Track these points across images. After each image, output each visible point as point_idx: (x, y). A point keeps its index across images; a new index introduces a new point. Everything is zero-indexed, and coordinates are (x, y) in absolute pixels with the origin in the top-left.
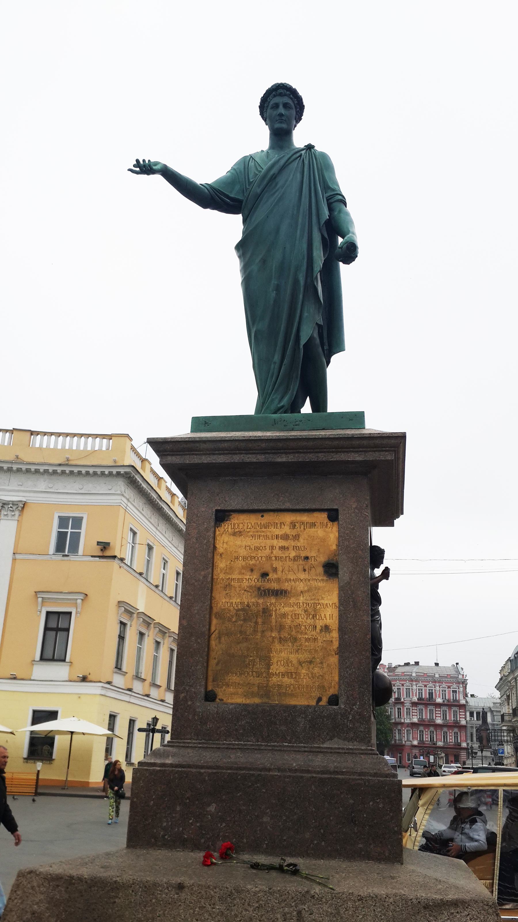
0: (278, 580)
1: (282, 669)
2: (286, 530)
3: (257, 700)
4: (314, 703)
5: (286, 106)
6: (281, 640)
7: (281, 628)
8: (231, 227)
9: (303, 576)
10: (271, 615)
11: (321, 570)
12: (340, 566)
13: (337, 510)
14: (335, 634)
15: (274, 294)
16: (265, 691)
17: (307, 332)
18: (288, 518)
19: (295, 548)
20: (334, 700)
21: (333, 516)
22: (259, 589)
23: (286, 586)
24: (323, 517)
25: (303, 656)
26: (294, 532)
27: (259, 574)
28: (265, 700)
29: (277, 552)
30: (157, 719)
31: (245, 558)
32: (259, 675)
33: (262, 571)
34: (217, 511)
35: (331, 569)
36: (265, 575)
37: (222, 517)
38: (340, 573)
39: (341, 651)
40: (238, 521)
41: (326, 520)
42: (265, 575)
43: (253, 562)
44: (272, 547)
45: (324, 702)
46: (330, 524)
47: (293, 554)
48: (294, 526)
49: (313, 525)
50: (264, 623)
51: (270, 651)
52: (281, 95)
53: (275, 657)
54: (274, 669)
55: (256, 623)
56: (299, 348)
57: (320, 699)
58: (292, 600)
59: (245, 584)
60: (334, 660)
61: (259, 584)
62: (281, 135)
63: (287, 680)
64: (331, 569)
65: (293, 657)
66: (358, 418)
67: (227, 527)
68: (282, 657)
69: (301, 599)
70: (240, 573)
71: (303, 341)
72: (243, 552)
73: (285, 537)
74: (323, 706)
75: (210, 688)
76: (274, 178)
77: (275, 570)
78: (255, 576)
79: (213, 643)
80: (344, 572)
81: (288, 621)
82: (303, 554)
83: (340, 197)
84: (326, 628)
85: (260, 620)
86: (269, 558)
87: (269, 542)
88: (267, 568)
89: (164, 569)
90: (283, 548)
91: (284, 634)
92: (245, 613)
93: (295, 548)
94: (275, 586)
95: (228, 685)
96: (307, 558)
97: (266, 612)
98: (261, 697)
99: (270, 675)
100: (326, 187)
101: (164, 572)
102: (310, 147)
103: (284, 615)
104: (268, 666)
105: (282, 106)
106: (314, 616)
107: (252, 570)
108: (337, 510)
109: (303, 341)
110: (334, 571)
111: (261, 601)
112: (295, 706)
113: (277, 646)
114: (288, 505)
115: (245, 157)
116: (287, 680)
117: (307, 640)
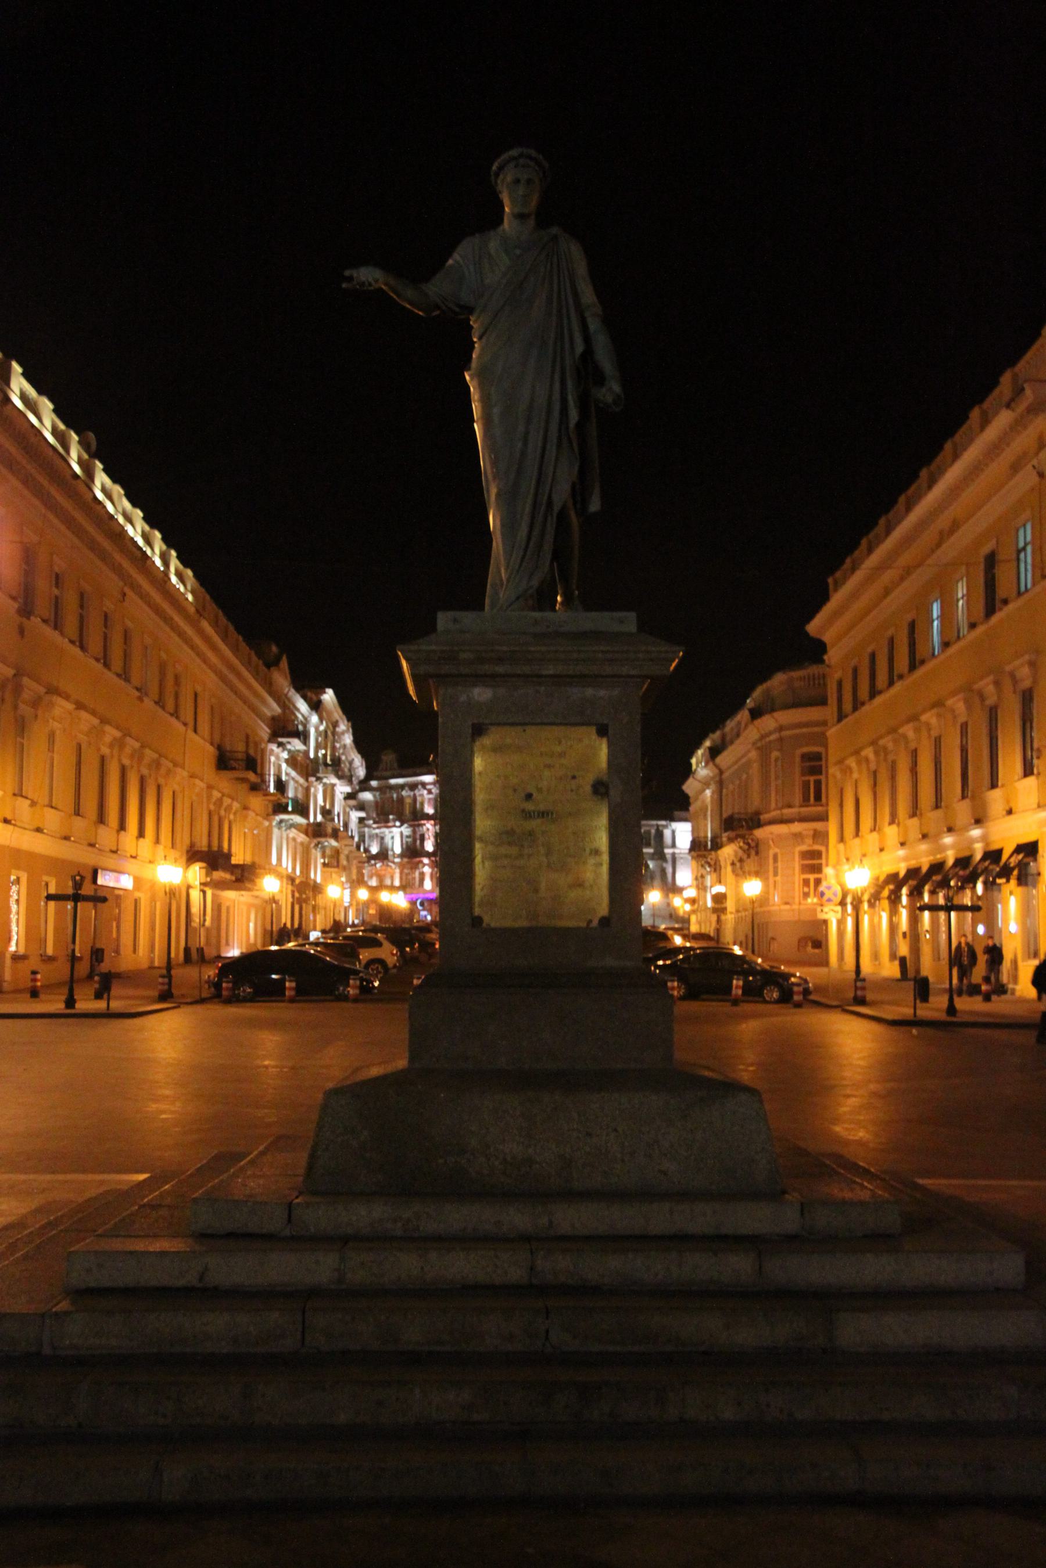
4: (585, 925)
12: (611, 786)
14: (605, 858)
15: (520, 445)
20: (605, 922)
27: (523, 795)
38: (612, 792)
41: (594, 736)
42: (529, 796)
45: (595, 923)
56: (552, 515)
57: (590, 921)
67: (486, 741)
80: (615, 793)
89: (57, 586)
94: (542, 807)
101: (56, 592)
107: (515, 790)
109: (556, 509)
110: (602, 790)
112: (568, 930)
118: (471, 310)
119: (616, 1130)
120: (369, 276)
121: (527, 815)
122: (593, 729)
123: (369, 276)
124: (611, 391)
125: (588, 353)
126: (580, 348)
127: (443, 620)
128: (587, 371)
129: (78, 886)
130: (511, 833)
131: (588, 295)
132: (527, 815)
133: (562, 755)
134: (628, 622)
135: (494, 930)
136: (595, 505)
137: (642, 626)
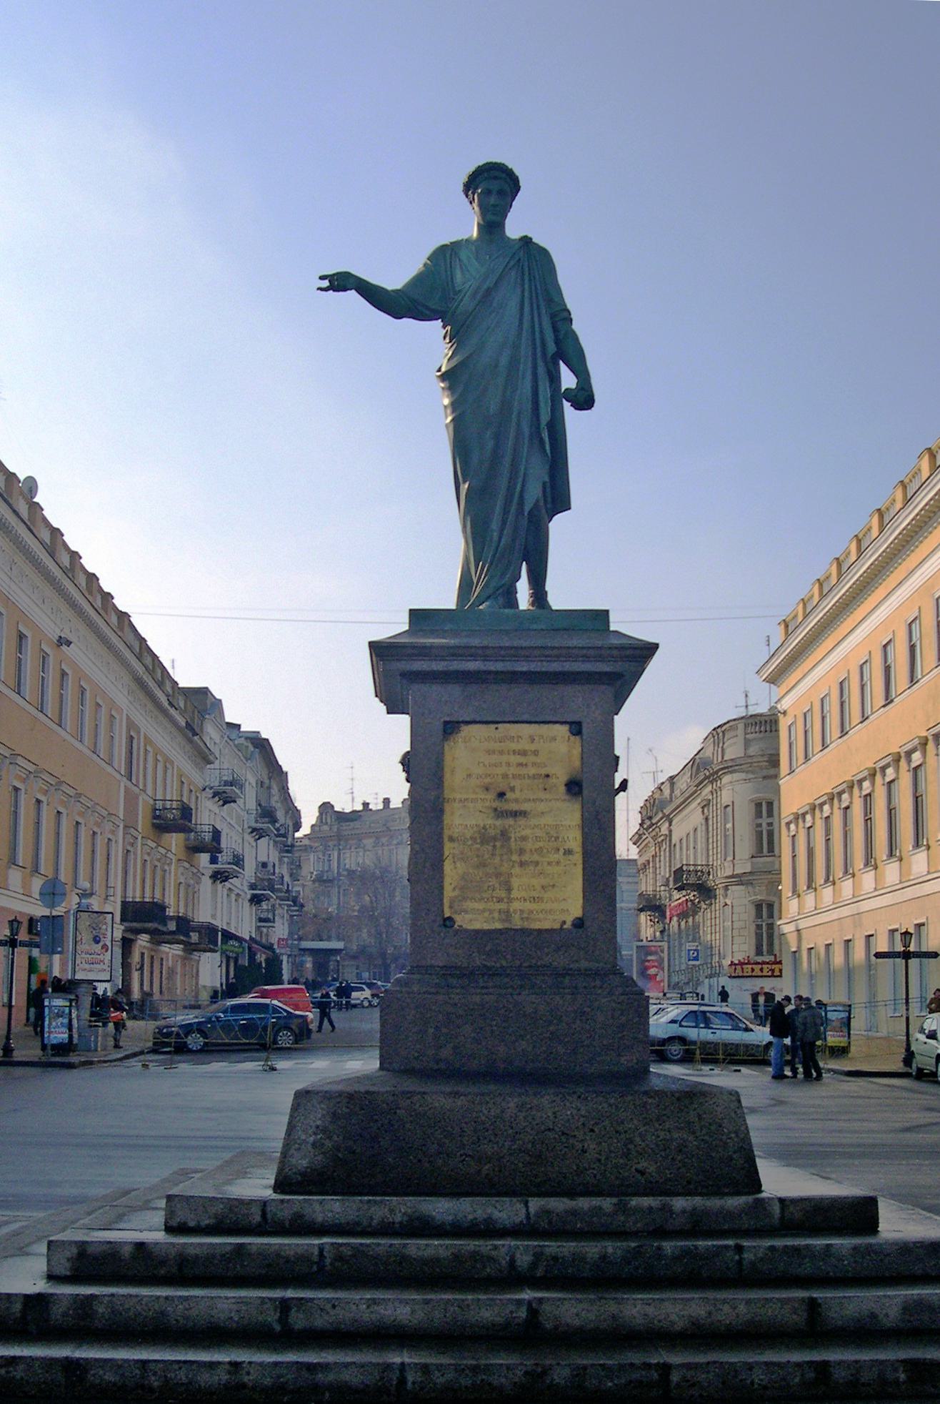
0: (516, 800)
1: (523, 894)
2: (524, 745)
3: (498, 926)
5: (501, 193)
6: (522, 864)
7: (521, 852)
8: (429, 343)
9: (542, 795)
10: (510, 838)
11: (562, 789)
12: (585, 785)
13: (579, 724)
14: (578, 858)
15: (490, 445)
16: (507, 915)
17: (534, 492)
18: (526, 730)
19: (534, 764)
20: (579, 923)
22: (496, 810)
23: (525, 807)
24: (563, 730)
25: (544, 881)
26: (533, 747)
28: (507, 925)
29: (513, 770)
30: (19, 922)
31: (479, 777)
32: (500, 900)
33: (499, 790)
34: (446, 723)
35: (574, 787)
36: (501, 795)
37: (450, 728)
42: (501, 795)
43: (488, 780)
44: (508, 764)
45: (568, 925)
46: (572, 738)
47: (533, 771)
48: (533, 740)
49: (554, 739)
50: (502, 846)
51: (510, 875)
52: (495, 178)
53: (515, 882)
54: (515, 894)
55: (494, 846)
57: (564, 922)
58: (533, 822)
59: (479, 805)
61: (495, 805)
62: (492, 225)
63: (528, 906)
64: (574, 787)
65: (535, 882)
66: (604, 615)
68: (521, 881)
69: (543, 821)
70: (474, 792)
71: (527, 508)
72: (479, 770)
73: (524, 753)
74: (569, 930)
75: (447, 914)
76: (488, 292)
77: (512, 789)
78: (491, 796)
79: (448, 866)
81: (529, 845)
82: (543, 771)
83: (565, 314)
84: (569, 852)
85: (498, 844)
86: (505, 776)
87: (504, 758)
88: (502, 786)
90: (520, 765)
91: (526, 857)
92: (484, 837)
93: (534, 764)
94: (514, 807)
95: (466, 912)
96: (548, 776)
97: (504, 834)
98: (503, 921)
99: (510, 900)
100: (550, 301)
102: (526, 241)
103: (524, 839)
104: (509, 890)
105: (494, 186)
106: (557, 838)
108: (579, 724)
109: (527, 508)
111: (499, 823)
113: (517, 870)
114: (526, 717)
115: (443, 248)
116: (528, 906)
117: (549, 863)
119: (592, 1131)
122: (566, 727)
129: (14, 932)
132: (499, 814)
133: (536, 753)
135: (466, 931)
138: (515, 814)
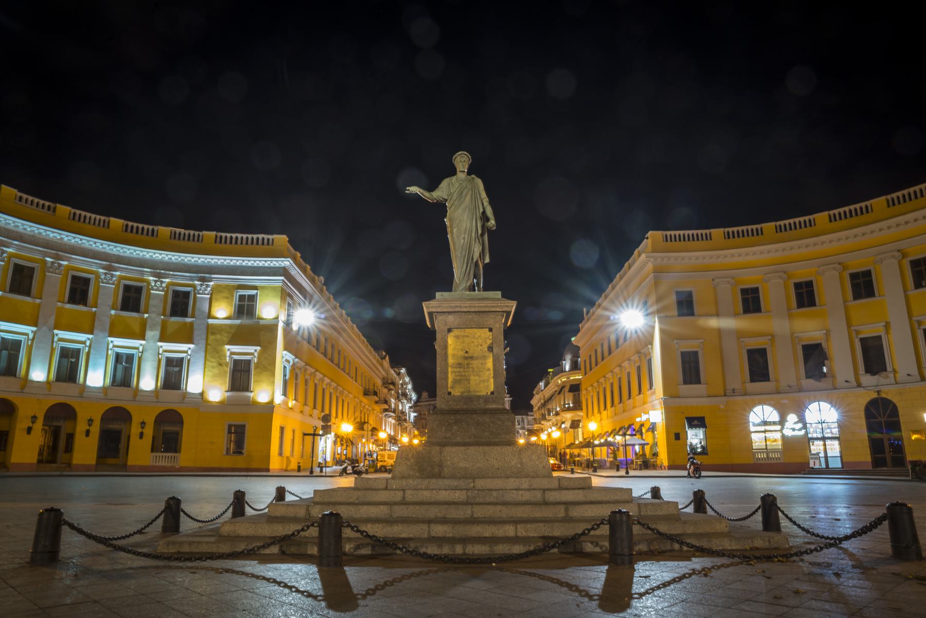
14: (492, 372)
20: (492, 393)
21: (491, 330)
39: (494, 377)
40: (456, 332)
60: (492, 380)
64: (490, 349)
67: (451, 334)
118: (446, 200)
120: (414, 189)
121: (466, 358)
123: (414, 189)
124: (492, 222)
125: (484, 213)
126: (481, 210)
127: (438, 295)
128: (485, 218)
130: (460, 364)
131: (484, 195)
134: (498, 294)
136: (487, 260)
137: (503, 296)
138: (472, 358)
